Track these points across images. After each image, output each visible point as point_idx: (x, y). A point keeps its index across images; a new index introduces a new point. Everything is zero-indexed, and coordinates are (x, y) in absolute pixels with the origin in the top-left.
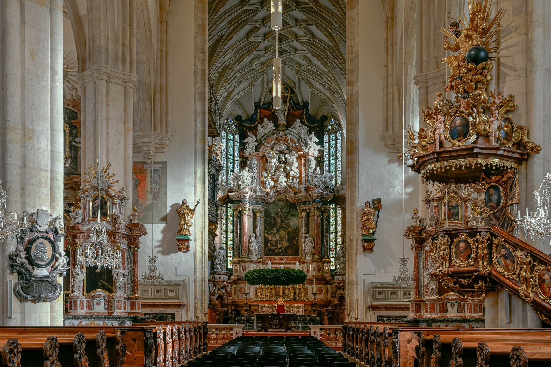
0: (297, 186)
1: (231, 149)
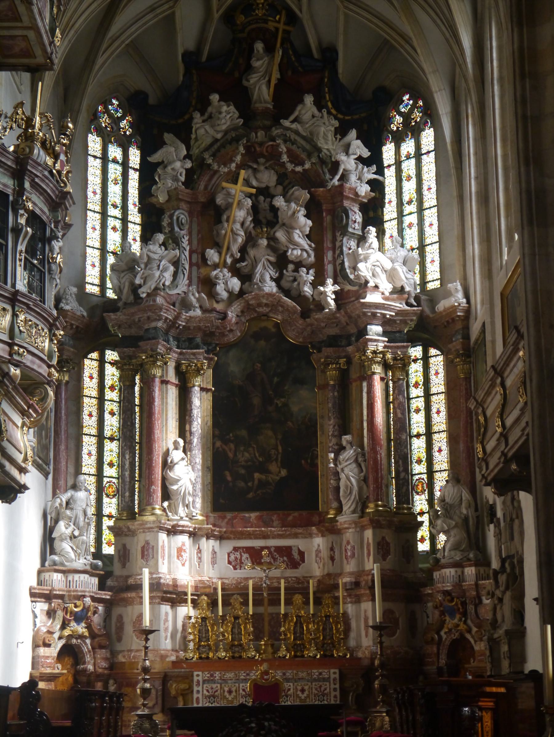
0: (308, 290)
1: (115, 191)
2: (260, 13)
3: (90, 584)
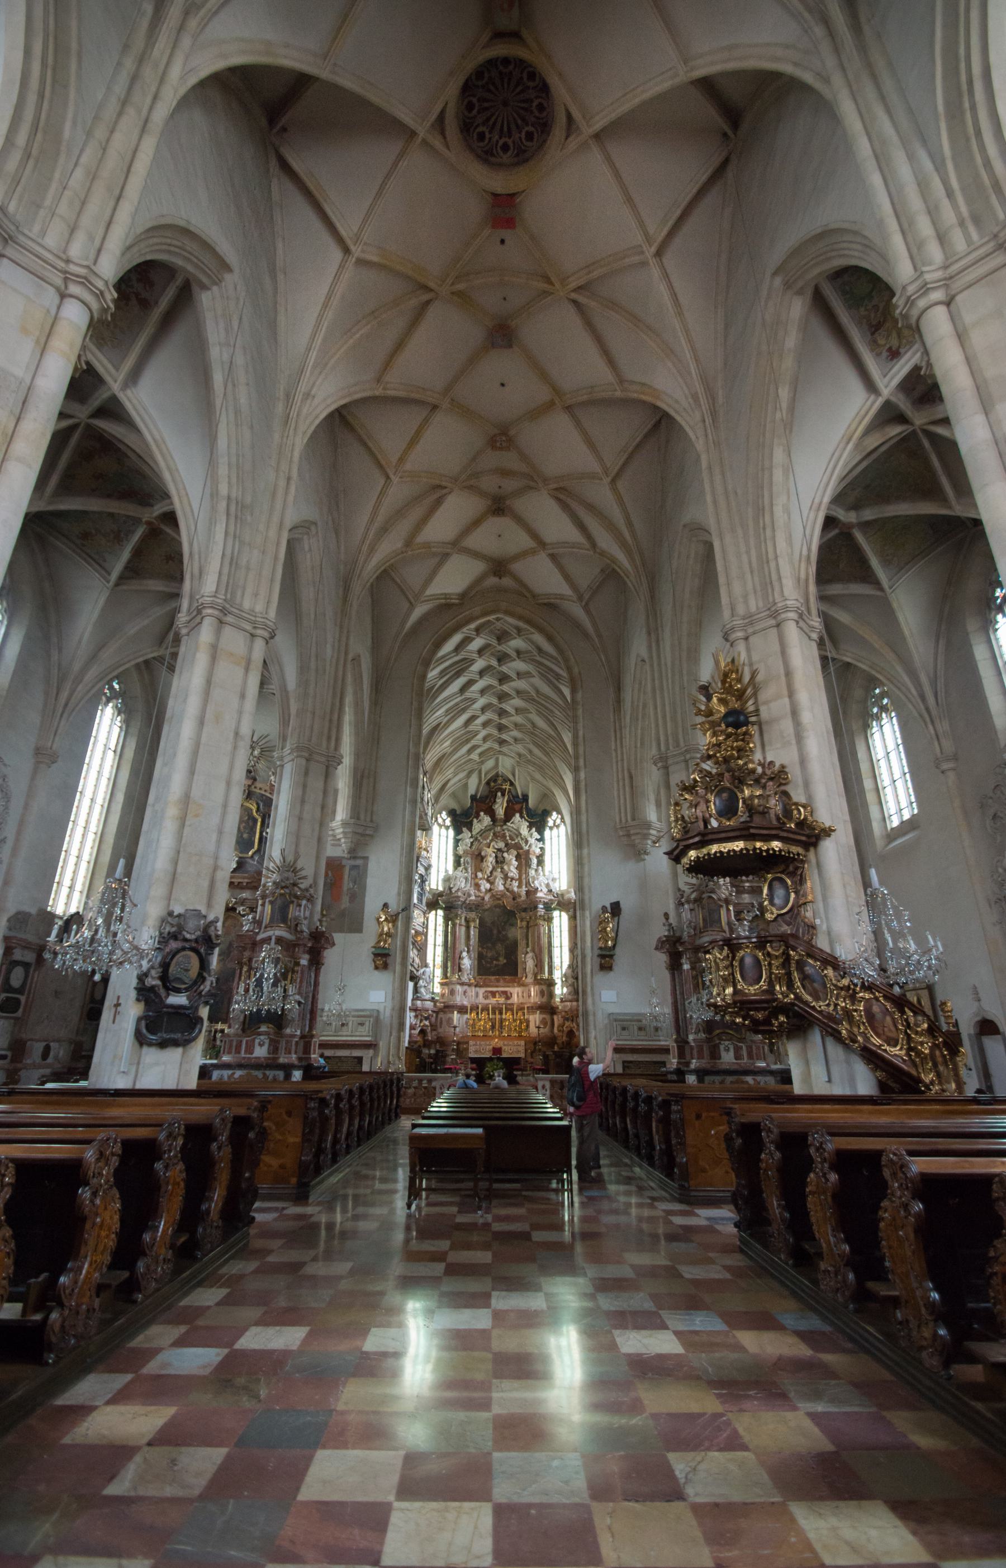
0: (516, 889)
2: (499, 782)
3: (429, 1005)
